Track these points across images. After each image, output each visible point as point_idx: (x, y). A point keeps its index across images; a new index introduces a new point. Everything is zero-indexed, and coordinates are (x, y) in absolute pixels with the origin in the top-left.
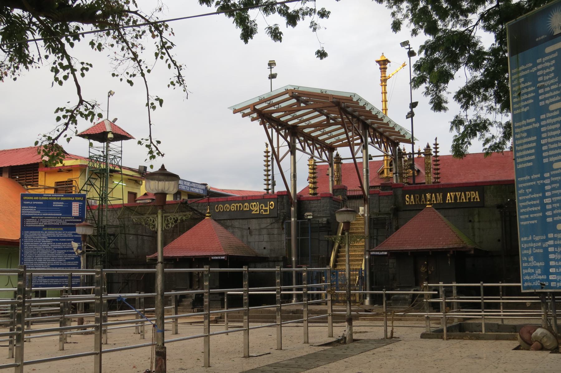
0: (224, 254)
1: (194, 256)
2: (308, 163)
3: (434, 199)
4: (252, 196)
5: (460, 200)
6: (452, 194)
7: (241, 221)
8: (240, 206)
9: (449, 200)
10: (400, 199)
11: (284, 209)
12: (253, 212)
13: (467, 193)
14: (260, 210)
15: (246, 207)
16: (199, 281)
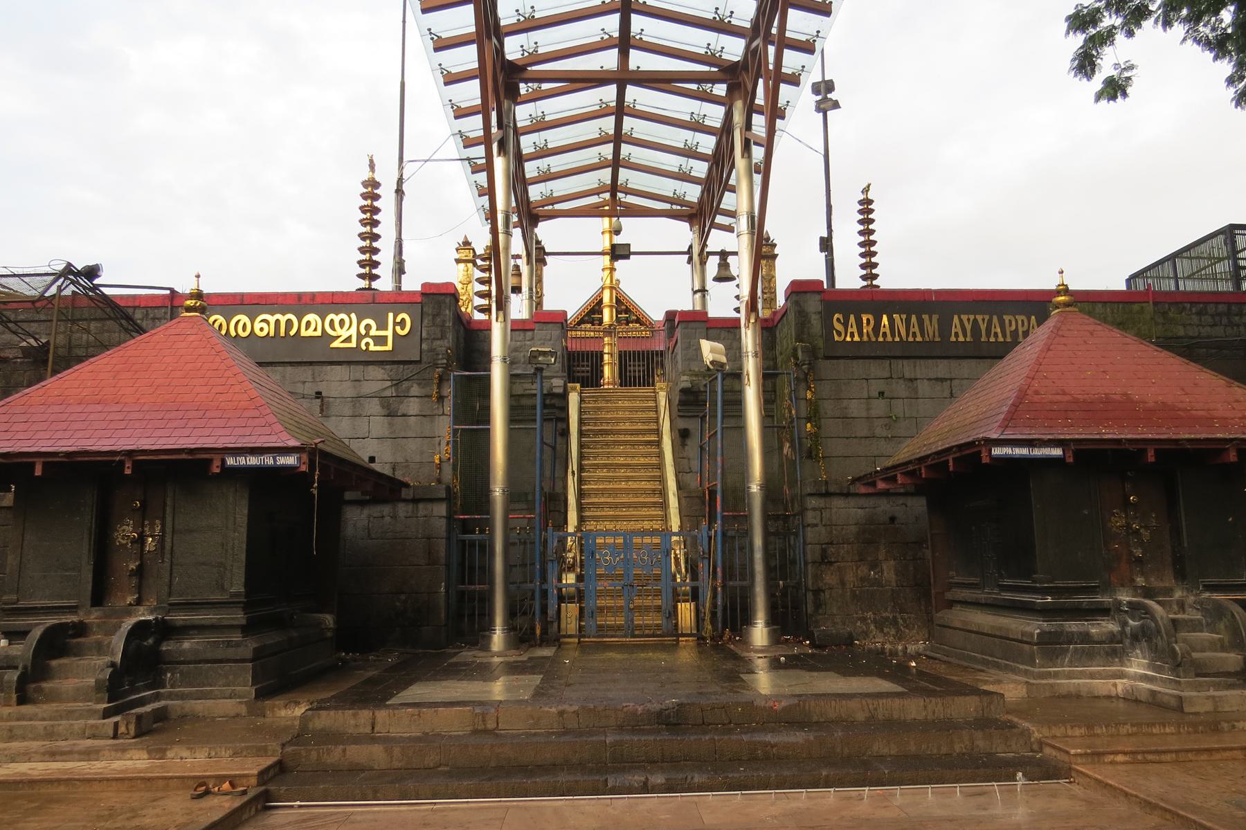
0: (293, 443)
1: (130, 453)
2: (457, 256)
3: (917, 329)
4: (333, 294)
5: (988, 335)
6: (964, 317)
7: (289, 369)
8: (289, 323)
9: (957, 335)
10: (816, 323)
11: (443, 337)
12: (336, 344)
13: (1007, 318)
14: (360, 337)
15: (312, 325)
16: (140, 572)
